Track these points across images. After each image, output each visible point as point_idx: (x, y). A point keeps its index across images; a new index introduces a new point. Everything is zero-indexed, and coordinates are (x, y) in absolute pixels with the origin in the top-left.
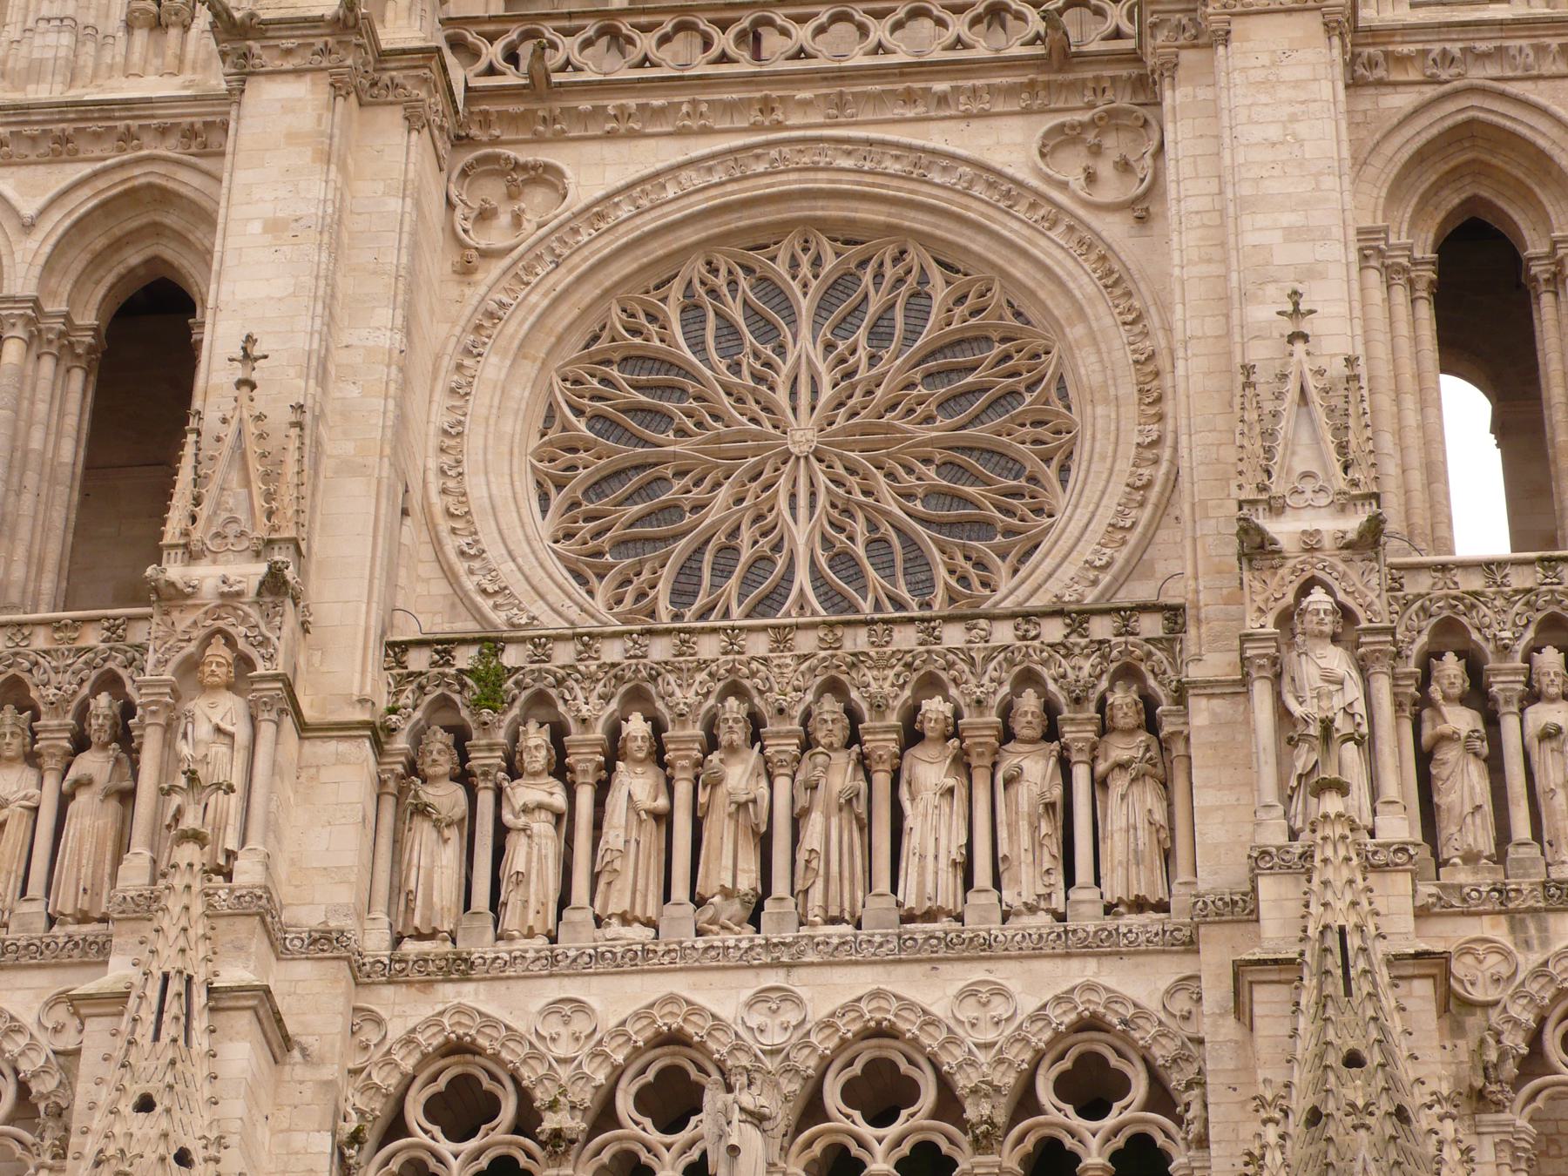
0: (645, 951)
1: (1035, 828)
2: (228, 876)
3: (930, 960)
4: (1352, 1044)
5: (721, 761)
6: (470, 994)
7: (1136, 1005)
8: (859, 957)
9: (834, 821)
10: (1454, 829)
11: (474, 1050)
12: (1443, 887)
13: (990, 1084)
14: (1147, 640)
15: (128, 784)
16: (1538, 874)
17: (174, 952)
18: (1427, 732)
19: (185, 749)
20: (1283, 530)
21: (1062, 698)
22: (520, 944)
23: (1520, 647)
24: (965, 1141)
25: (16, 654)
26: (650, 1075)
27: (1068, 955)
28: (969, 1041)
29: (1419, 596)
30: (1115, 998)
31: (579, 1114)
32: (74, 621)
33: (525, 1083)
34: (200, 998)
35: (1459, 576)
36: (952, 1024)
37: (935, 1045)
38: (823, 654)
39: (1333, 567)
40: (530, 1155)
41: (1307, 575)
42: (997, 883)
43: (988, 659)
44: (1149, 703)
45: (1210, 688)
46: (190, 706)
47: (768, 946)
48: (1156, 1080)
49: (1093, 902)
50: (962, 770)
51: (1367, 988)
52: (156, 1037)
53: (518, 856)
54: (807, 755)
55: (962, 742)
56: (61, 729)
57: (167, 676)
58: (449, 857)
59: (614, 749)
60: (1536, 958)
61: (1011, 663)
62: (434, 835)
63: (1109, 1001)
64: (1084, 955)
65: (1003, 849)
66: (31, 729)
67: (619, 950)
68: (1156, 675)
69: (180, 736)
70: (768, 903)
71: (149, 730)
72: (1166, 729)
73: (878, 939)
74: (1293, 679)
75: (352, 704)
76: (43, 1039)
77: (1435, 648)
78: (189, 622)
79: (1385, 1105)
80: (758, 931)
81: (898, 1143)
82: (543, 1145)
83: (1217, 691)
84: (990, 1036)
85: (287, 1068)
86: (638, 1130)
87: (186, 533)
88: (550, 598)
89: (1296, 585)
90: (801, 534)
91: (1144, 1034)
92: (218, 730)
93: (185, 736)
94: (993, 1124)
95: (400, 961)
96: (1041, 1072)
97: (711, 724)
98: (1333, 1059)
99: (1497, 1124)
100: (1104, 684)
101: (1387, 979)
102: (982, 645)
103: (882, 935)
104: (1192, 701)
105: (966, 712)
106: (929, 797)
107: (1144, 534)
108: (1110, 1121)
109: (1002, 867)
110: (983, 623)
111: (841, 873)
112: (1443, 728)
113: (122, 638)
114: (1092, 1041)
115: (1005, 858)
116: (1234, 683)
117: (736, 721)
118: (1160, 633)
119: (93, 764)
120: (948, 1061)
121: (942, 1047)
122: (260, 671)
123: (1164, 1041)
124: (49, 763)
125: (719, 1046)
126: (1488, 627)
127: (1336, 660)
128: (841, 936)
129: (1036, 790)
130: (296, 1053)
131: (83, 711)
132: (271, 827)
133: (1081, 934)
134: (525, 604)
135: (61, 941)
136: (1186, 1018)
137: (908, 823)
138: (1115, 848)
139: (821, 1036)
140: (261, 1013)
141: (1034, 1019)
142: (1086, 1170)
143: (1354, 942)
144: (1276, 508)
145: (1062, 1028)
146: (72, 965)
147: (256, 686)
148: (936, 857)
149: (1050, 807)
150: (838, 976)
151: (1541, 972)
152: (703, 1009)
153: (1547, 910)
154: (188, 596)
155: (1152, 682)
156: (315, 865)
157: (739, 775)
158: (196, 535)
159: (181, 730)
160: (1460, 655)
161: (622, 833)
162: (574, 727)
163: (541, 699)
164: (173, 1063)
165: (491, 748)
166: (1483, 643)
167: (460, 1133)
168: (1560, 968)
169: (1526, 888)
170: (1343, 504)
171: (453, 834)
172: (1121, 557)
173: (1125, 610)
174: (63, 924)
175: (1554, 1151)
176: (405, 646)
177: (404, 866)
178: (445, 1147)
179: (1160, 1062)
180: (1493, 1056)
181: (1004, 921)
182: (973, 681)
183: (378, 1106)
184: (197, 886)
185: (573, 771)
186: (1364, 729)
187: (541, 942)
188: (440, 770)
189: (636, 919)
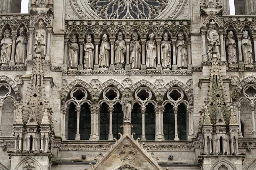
0: (107, 72)
1: (167, 55)
2: (44, 59)
3: (151, 75)
4: (218, 93)
5: (118, 42)
6: (80, 77)
7: (182, 83)
8: (140, 74)
9: (136, 53)
10: (231, 58)
11: (81, 86)
12: (229, 68)
13: (160, 95)
14: (185, 26)
15: (26, 42)
16: (243, 66)
17: (38, 71)
18: (227, 43)
19: (37, 38)
20: (207, 11)
21: (171, 34)
22: (88, 70)
23: (242, 30)
24: (156, 103)
25: (8, 20)
26: (108, 91)
27: (172, 75)
28: (157, 88)
29: (227, 22)
30: (179, 82)
31: (97, 97)
32: (17, 15)
33: (89, 92)
34: (42, 79)
35: (233, 19)
36: (155, 85)
37: (152, 88)
38: (134, 25)
39: (215, 17)
40: (90, 103)
41: (211, 18)
42: (161, 63)
43: (160, 28)
44: (184, 36)
45: (195, 35)
46: (37, 31)
47: (126, 72)
48: (185, 95)
49: (176, 67)
50: (156, 45)
51: (220, 85)
52: (36, 85)
53: (87, 56)
54: (132, 41)
55: (156, 41)
56: (15, 33)
57: (33, 26)
58: (76, 55)
59: (101, 39)
60: (242, 79)
61: (163, 28)
62: (74, 52)
63: (178, 83)
64: (175, 75)
65: (162, 58)
66: (10, 32)
67: (103, 72)
68: (186, 32)
69: (35, 36)
70: (126, 65)
71: (31, 35)
72: (187, 40)
73: (143, 72)
74: (208, 35)
75: (61, 31)
76: (15, 82)
77: (228, 30)
78: (36, 17)
79: (223, 103)
80: (125, 70)
81: (146, 103)
82: (92, 102)
83: (196, 35)
84: (160, 87)
85: (53, 89)
86: (106, 100)
87: (35, 3)
88: (89, 12)
89: (209, 20)
90: (128, 4)
91: (183, 88)
92: (42, 35)
93: (36, 36)
94: (161, 101)
95: (69, 72)
96: (168, 93)
97: (117, 36)
98: (215, 96)
99: (236, 104)
100: (178, 32)
101: (223, 83)
102: (159, 25)
103: (144, 71)
104: (192, 36)
105: (157, 36)
106: (151, 49)
107: (182, 7)
108: (178, 101)
109: (162, 61)
110: (159, 22)
111: (137, 61)
112: (230, 43)
113: (24, 18)
114: (175, 88)
115: (163, 59)
116: (198, 34)
117: (121, 36)
118: (186, 25)
119: (20, 38)
120: (154, 91)
121: (153, 89)
122: (48, 26)
123: (186, 89)
124: (13, 38)
125: (119, 87)
126: (237, 27)
127: (215, 32)
128: (137, 71)
129: (167, 49)
130: (54, 86)
131: (19, 30)
132: (50, 51)
133: (174, 72)
134: (85, 13)
135: (17, 67)
136: (190, 86)
137: (147, 53)
138: (179, 59)
139: (134, 86)
140: (51, 81)
141: (167, 85)
142: (174, 108)
143: (218, 77)
144: (206, 7)
145: (171, 87)
146: (19, 71)
147: (47, 28)
148: (152, 59)
149: (169, 52)
150: (137, 77)
151: (243, 81)
152: (116, 81)
153: (244, 72)
154: (36, 13)
155: (185, 32)
156: (56, 56)
157: (121, 44)
158: (37, 3)
159: (36, 35)
160: (232, 31)
161: (103, 53)
162: (95, 35)
163: (90, 30)
164: (39, 89)
165: (82, 38)
166: (236, 30)
167: (78, 99)
168: (246, 81)
169: (241, 68)
170: (216, 8)
171: (76, 52)
172: (179, 10)
173: (181, 21)
174: (17, 64)
175: (243, 107)
176: (68, 21)
177: (69, 57)
178: (77, 101)
179: (186, 92)
180: (236, 94)
181: (162, 69)
182: (158, 31)
183: (66, 94)
184: (41, 61)
185: (95, 42)
186: (219, 43)
187: (91, 70)
188: (74, 41)
189: (106, 67)
